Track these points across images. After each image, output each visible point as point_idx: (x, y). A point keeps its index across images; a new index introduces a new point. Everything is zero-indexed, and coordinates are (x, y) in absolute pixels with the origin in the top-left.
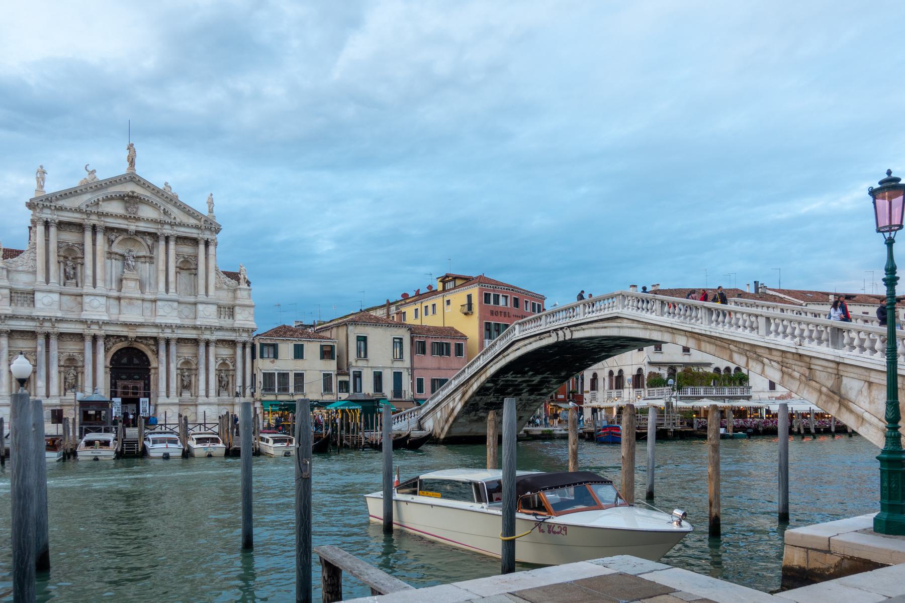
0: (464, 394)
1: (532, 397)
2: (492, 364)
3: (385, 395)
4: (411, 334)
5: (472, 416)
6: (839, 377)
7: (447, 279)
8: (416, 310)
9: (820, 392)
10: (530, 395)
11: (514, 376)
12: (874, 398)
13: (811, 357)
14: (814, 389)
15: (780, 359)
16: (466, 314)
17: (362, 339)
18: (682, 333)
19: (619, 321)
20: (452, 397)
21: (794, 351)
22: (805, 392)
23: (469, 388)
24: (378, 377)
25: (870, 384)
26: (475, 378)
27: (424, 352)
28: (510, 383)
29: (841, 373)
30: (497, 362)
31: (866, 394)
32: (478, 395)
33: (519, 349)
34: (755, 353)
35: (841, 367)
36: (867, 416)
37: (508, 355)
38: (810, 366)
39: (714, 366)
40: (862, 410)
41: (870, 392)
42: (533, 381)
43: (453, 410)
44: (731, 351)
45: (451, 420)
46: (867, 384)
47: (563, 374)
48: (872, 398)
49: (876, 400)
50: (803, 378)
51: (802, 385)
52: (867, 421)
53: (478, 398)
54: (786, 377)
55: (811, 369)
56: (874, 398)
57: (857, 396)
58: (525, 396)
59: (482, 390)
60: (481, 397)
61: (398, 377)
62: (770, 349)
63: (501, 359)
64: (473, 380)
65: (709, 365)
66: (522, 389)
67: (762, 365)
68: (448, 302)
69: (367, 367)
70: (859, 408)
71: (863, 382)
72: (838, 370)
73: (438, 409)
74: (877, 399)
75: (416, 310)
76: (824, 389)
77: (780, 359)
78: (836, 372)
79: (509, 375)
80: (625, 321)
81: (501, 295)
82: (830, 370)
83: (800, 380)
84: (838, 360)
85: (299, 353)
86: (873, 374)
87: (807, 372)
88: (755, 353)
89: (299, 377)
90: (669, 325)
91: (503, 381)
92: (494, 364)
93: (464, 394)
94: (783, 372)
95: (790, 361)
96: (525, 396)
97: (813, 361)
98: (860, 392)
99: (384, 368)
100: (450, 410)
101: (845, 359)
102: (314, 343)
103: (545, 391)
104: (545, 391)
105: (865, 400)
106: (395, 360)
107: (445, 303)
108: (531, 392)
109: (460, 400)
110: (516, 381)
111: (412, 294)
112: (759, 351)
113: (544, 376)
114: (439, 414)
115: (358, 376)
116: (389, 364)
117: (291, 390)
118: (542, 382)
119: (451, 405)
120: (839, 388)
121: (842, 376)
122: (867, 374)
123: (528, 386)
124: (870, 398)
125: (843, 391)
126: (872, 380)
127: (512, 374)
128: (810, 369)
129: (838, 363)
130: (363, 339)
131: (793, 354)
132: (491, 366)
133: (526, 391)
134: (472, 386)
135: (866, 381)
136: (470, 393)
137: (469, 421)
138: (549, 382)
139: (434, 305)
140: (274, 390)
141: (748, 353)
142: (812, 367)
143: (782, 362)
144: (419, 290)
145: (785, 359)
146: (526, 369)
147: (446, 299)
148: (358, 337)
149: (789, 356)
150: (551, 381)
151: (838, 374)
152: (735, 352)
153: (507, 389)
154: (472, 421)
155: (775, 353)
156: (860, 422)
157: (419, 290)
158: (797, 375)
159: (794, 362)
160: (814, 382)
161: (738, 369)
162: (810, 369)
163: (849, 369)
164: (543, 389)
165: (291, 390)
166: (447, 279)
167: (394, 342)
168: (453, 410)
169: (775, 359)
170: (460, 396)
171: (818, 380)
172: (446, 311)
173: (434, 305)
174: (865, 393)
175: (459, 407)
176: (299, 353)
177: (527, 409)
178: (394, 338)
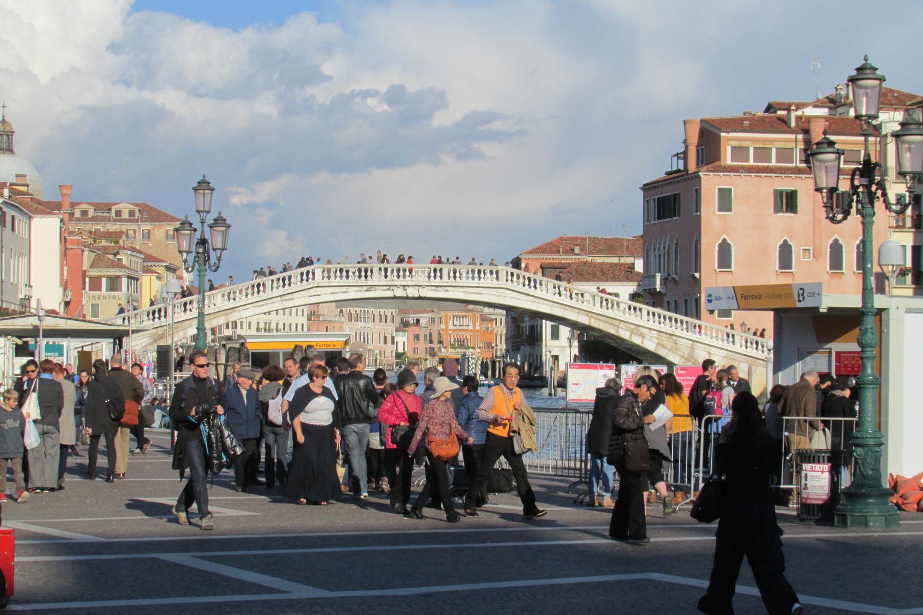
6: (692, 348)
29: (694, 347)
30: (262, 305)
35: (695, 344)
37: (292, 299)
78: (691, 346)
82: (688, 345)
86: (713, 348)
92: (254, 307)
97: (679, 339)
120: (693, 355)
125: (695, 357)
126: (711, 352)
128: (676, 343)
129: (694, 341)
142: (677, 342)
152: (622, 328)
155: (652, 332)
162: (676, 343)
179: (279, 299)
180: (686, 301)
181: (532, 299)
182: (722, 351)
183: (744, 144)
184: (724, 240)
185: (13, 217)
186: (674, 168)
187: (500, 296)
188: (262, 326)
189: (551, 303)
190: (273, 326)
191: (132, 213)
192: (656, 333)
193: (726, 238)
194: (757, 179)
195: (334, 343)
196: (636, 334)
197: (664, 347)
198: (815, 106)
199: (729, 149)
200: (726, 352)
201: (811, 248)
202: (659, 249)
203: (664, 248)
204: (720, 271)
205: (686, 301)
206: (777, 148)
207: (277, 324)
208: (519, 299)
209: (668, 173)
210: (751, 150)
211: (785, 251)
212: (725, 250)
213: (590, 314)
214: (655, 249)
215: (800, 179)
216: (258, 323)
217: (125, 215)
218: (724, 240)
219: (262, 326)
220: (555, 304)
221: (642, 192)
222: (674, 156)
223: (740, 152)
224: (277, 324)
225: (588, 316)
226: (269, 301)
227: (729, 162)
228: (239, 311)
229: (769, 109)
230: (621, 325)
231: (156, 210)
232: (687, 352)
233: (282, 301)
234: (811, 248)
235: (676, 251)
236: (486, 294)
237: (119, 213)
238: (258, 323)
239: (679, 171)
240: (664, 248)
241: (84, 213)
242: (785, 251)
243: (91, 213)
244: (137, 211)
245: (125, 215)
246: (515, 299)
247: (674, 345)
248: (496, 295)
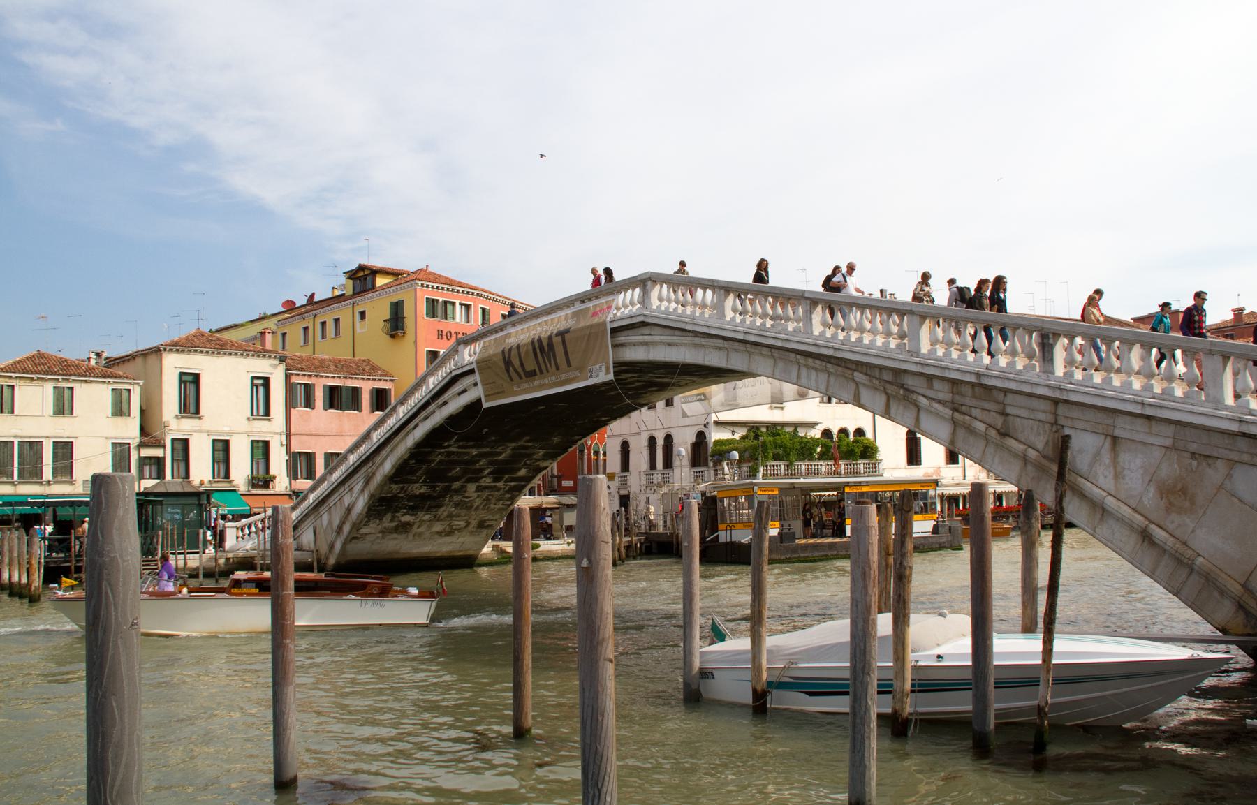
0: (367, 483)
1: (500, 484)
3: (235, 483)
4: (287, 370)
5: (387, 522)
7: (361, 274)
8: (306, 329)
9: (1025, 459)
10: (496, 480)
11: (461, 443)
12: (1124, 469)
13: (1006, 391)
14: (1014, 454)
15: (948, 397)
16: (392, 336)
17: (190, 378)
18: (765, 351)
19: (646, 330)
20: (346, 485)
21: (973, 379)
22: (996, 460)
23: (378, 468)
24: (222, 450)
25: (1115, 439)
26: (388, 449)
27: (309, 403)
28: (456, 458)
29: (1062, 421)
30: (426, 418)
31: (1107, 461)
32: (396, 483)
33: (464, 391)
34: (902, 386)
35: (1062, 410)
36: (1110, 502)
37: (445, 403)
38: (1004, 408)
39: (820, 428)
40: (1100, 491)
42: (500, 453)
43: (349, 510)
44: (856, 382)
45: (347, 528)
46: (1109, 439)
47: (556, 440)
48: (1119, 469)
49: (1126, 472)
50: (993, 433)
51: (991, 449)
52: (1110, 514)
53: (395, 488)
54: (961, 433)
55: (1007, 415)
56: (1124, 469)
57: (1091, 465)
58: (487, 481)
59: (402, 472)
60: (402, 485)
61: (261, 450)
62: (930, 378)
63: (434, 412)
64: (384, 453)
65: (813, 425)
66: (481, 470)
67: (914, 410)
68: (363, 314)
69: (200, 431)
70: (1096, 490)
71: (1103, 437)
72: (1056, 415)
73: (323, 509)
74: (1129, 469)
75: (306, 329)
76: (1032, 454)
77: (948, 397)
79: (452, 442)
80: (657, 330)
81: (457, 302)
82: (1042, 416)
83: (986, 437)
84: (1057, 395)
85: (63, 406)
86: (1121, 421)
87: (999, 421)
88: (902, 386)
89: (64, 451)
90: (741, 336)
91: (440, 454)
92: (421, 421)
93: (367, 483)
94: (955, 423)
95: (968, 401)
96: (487, 481)
97: (1010, 398)
98: (1097, 455)
99: (232, 433)
100: (344, 510)
101: (1071, 394)
102: (94, 385)
103: (523, 472)
104: (523, 472)
105: (1107, 473)
106: (253, 416)
107: (357, 316)
108: (497, 475)
109: (362, 491)
110: (468, 454)
111: (301, 301)
112: (910, 382)
113: (519, 443)
114: (325, 518)
115: (183, 448)
116: (244, 425)
117: (48, 473)
118: (516, 459)
119: (347, 500)
121: (1063, 426)
122: (1109, 422)
123: (491, 463)
124: (1115, 467)
126: (1117, 433)
127: (457, 441)
128: (1004, 414)
129: (1056, 402)
130: (191, 382)
131: (972, 385)
132: (416, 426)
133: (489, 474)
134: (382, 463)
135: (1107, 435)
136: (378, 479)
137: (382, 532)
138: (529, 456)
139: (337, 321)
140: (12, 476)
141: (888, 386)
142: (1009, 410)
143: (953, 402)
144: (312, 296)
145: (957, 398)
146: (486, 430)
147: (358, 309)
148: (182, 374)
150: (534, 454)
151: (1056, 423)
153: (450, 470)
154: (384, 532)
155: (937, 385)
156: (1098, 516)
157: (312, 296)
158: (980, 427)
159: (973, 402)
160: (1013, 441)
161: (860, 432)
162: (1004, 414)
163: (1076, 413)
164: (519, 469)
165: (48, 473)
166: (361, 274)
167: (253, 385)
168: (349, 510)
169: (941, 396)
170: (361, 483)
171: (1020, 436)
172: (358, 330)
173: (337, 321)
174: (1106, 458)
175: (361, 505)
176: (63, 406)
177: (492, 506)
178: (254, 378)
182: (1156, 427)
189: (719, 343)
200: (1169, 430)
246: (669, 344)
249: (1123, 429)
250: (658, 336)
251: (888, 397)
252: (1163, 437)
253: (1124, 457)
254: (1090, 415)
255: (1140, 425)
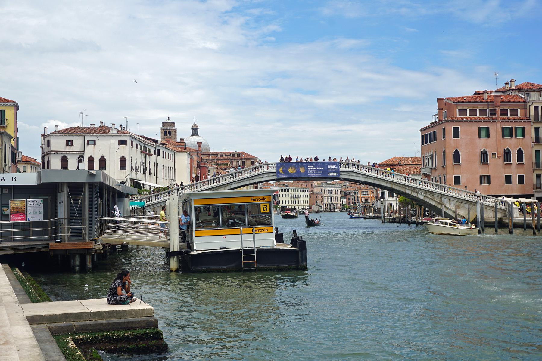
2: (236, 182)
6: (441, 198)
13: (434, 192)
35: (442, 196)
41: (449, 202)
62: (421, 189)
80: (353, 173)
86: (451, 198)
97: (435, 194)
128: (433, 196)
129: (442, 194)
131: (428, 191)
149: (427, 192)
152: (407, 189)
155: (422, 190)
163: (445, 196)
179: (248, 179)
180: (440, 178)
181: (365, 176)
182: (456, 199)
183: (464, 108)
184: (457, 150)
185: (163, 152)
186: (434, 121)
187: (350, 175)
188: (292, 196)
190: (297, 196)
191: (238, 155)
192: (423, 191)
193: (457, 149)
194: (470, 123)
195: (265, 197)
196: (414, 192)
197: (428, 197)
198: (496, 92)
199: (458, 110)
200: (457, 199)
201: (496, 153)
202: (428, 156)
203: (430, 155)
204: (455, 164)
205: (440, 178)
206: (479, 109)
207: (298, 195)
208: (359, 177)
209: (431, 124)
210: (468, 110)
211: (484, 155)
212: (457, 155)
213: (392, 183)
214: (426, 156)
215: (490, 123)
216: (291, 195)
217: (236, 156)
218: (457, 150)
219: (292, 196)
220: (375, 179)
221: (420, 132)
222: (434, 116)
223: (462, 112)
224: (298, 195)
225: (391, 184)
226: (244, 180)
227: (458, 116)
228: (230, 185)
229: (475, 94)
230: (407, 188)
231: (248, 154)
232: (439, 200)
233: (249, 180)
234: (496, 153)
235: (435, 156)
236: (343, 175)
237: (234, 155)
238: (291, 195)
239: (436, 122)
240: (430, 155)
241: (221, 156)
242: (484, 155)
243: (224, 156)
244: (240, 154)
245: (236, 156)
247: (432, 196)
248: (348, 175)
249: (451, 199)
250: (354, 174)
251: (412, 191)
252: (456, 200)
253: (451, 202)
254: (446, 196)
255: (453, 198)
